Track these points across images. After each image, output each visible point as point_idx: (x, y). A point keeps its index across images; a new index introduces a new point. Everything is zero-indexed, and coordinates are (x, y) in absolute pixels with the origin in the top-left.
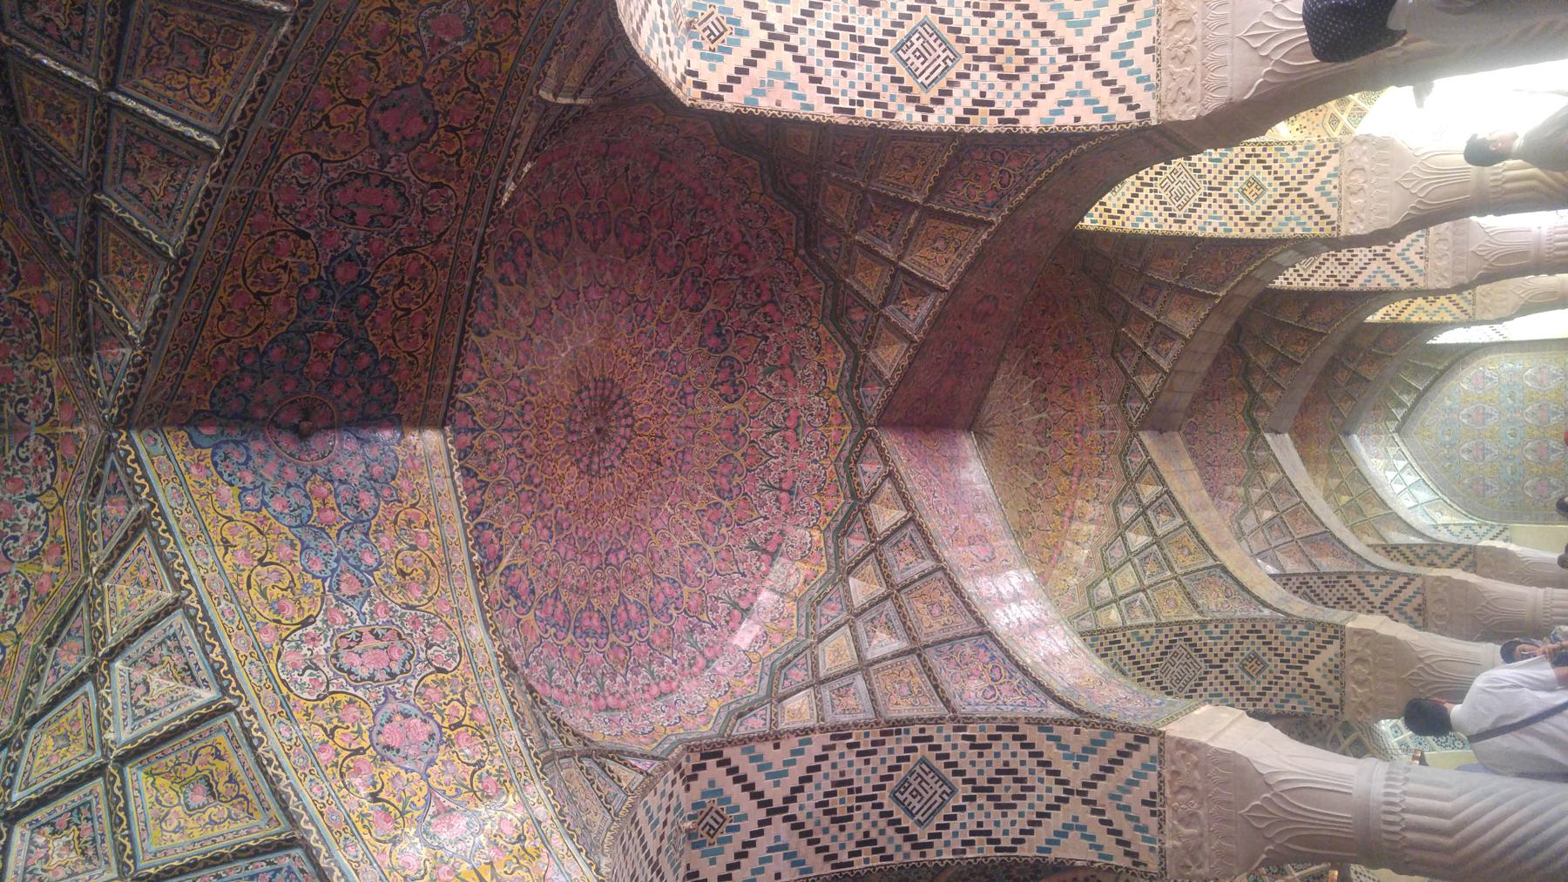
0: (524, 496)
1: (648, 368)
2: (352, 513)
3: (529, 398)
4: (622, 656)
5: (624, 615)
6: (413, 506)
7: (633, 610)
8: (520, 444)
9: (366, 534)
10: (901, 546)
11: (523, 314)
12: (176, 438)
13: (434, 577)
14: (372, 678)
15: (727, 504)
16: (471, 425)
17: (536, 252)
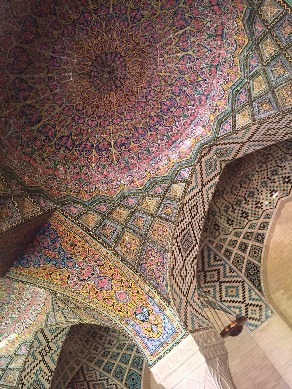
0: (102, 123)
1: (109, 31)
2: (57, 250)
3: (75, 105)
4: (171, 120)
5: (166, 107)
6: (67, 236)
7: (168, 103)
8: (87, 115)
9: (64, 251)
10: (284, 26)
11: (44, 94)
12: (12, 269)
13: (86, 247)
14: (89, 278)
15: (188, 28)
16: (66, 138)
17: (23, 76)
